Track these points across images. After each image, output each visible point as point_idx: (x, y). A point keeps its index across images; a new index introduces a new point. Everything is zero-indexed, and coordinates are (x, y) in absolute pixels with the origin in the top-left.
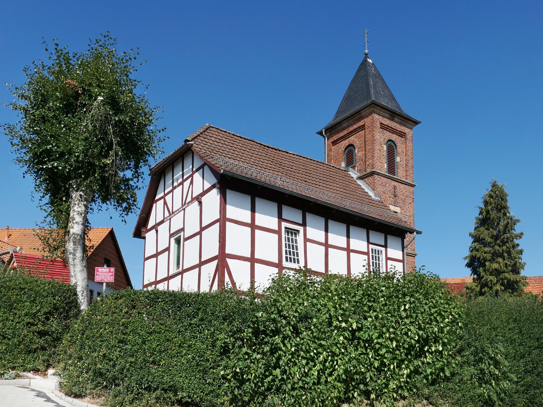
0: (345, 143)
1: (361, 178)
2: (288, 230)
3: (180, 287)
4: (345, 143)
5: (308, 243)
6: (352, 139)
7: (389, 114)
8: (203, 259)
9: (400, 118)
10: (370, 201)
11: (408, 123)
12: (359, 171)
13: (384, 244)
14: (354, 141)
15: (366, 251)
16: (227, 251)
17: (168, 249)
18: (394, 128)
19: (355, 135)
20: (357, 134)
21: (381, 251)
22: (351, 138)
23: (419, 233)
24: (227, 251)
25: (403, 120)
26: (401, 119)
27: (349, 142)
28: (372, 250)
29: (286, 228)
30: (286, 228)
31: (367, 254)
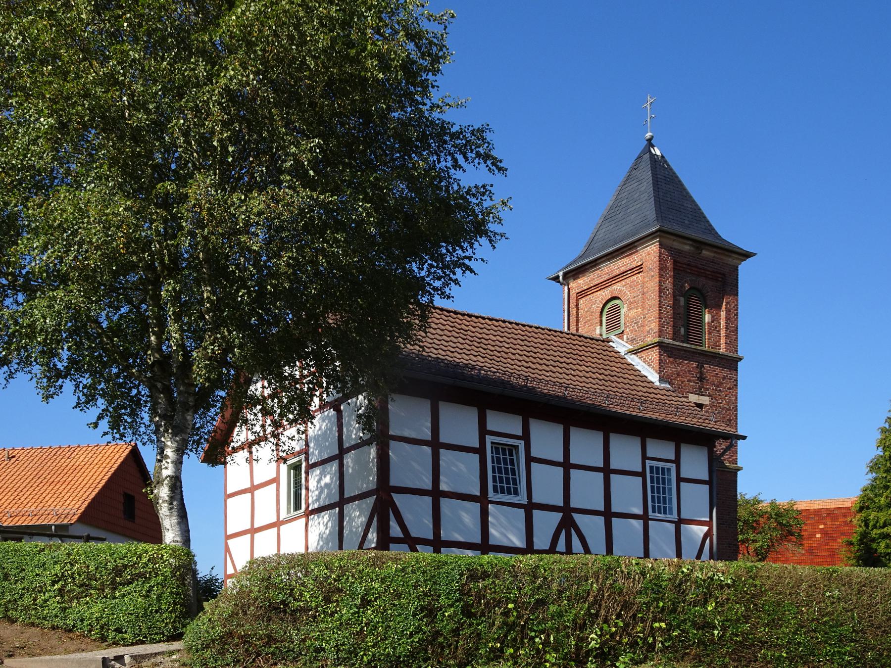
0: (606, 294)
1: (631, 352)
2: (496, 446)
3: (309, 533)
4: (606, 294)
5: (533, 465)
6: (617, 288)
7: (691, 245)
8: (256, 483)
9: (715, 250)
10: (652, 390)
11: (730, 256)
12: (631, 341)
13: (673, 458)
14: (620, 291)
15: (640, 470)
16: (393, 482)
17: (276, 480)
18: (701, 266)
19: (623, 282)
20: (628, 281)
21: (669, 470)
22: (615, 287)
23: (744, 438)
24: (393, 482)
25: (719, 253)
26: (715, 252)
27: (611, 292)
28: (651, 468)
29: (492, 443)
30: (492, 443)
31: (642, 474)
